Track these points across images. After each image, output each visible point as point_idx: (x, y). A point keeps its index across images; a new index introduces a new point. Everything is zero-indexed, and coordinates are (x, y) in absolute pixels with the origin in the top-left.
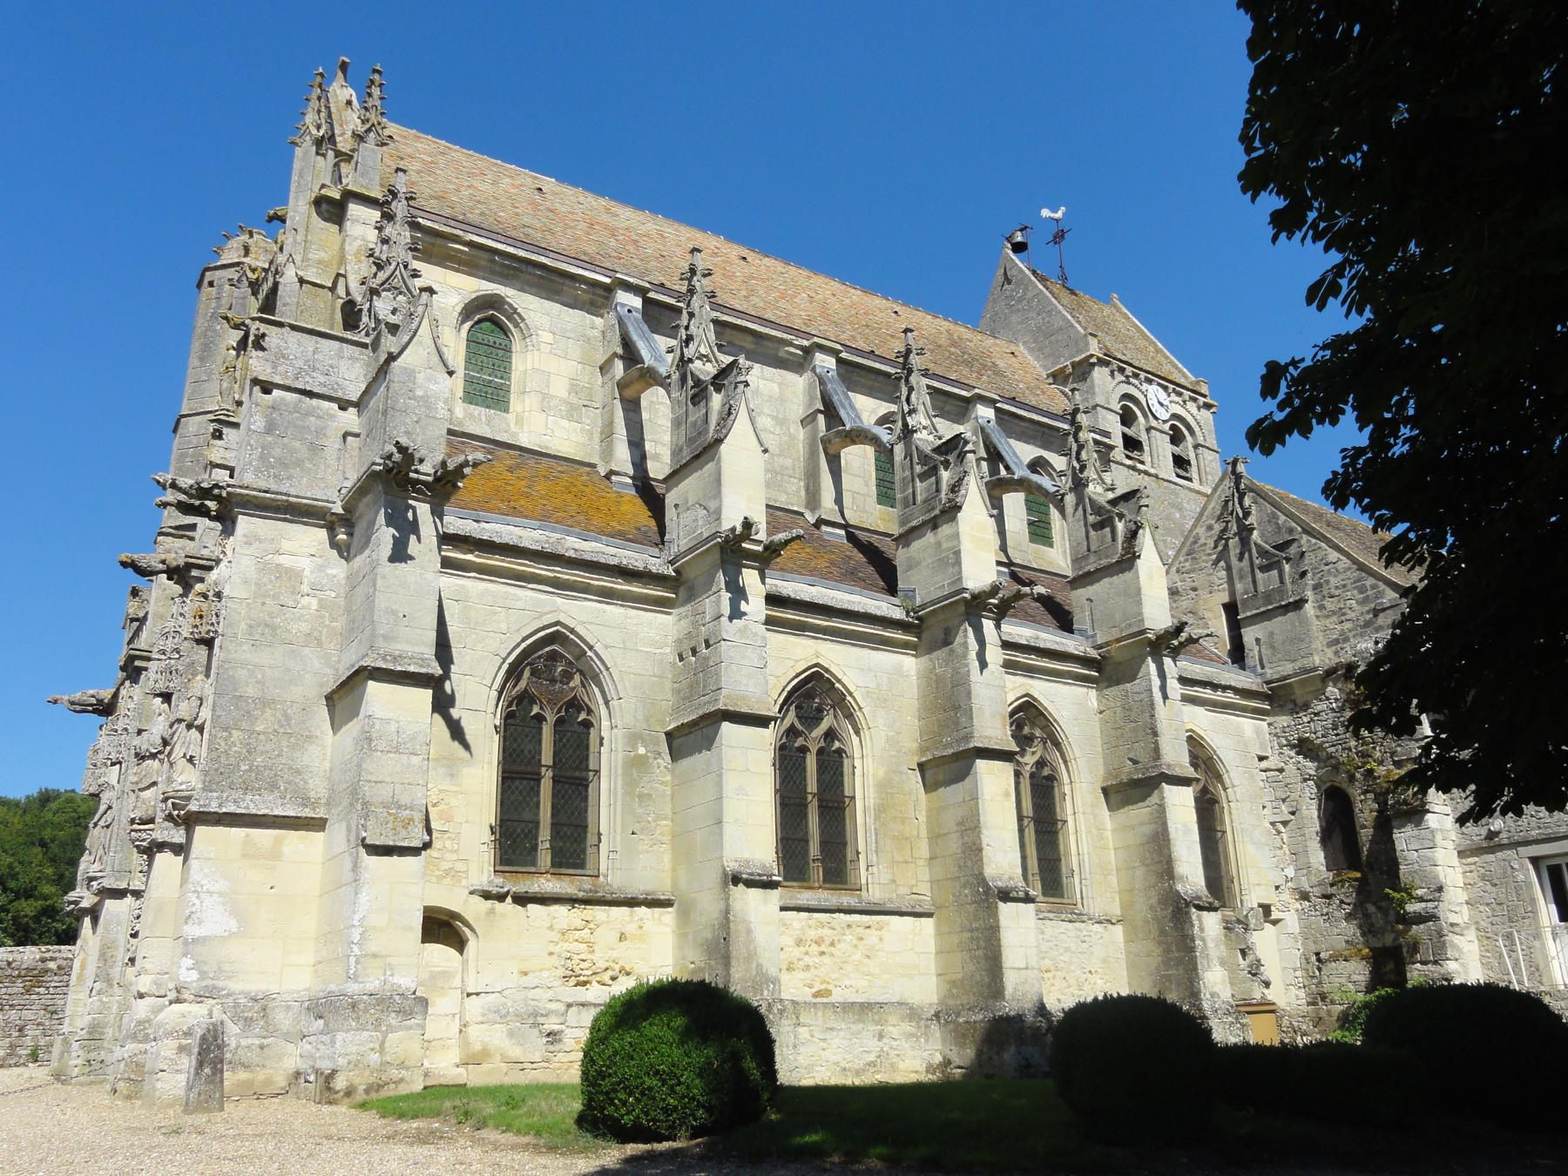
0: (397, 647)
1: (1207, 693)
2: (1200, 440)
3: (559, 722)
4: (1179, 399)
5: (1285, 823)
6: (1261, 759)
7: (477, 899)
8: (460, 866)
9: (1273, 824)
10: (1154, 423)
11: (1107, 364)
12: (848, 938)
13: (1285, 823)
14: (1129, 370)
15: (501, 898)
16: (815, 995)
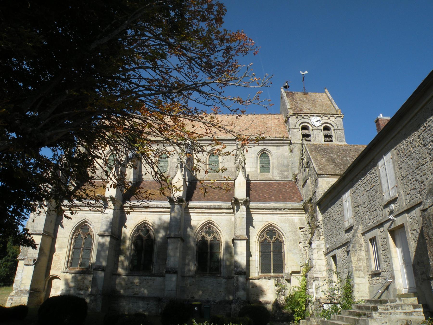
0: (37, 229)
1: (278, 211)
2: (336, 128)
3: (86, 238)
4: (326, 118)
5: (307, 247)
6: (301, 228)
7: (62, 273)
8: (60, 267)
9: (304, 247)
10: (315, 128)
11: (295, 115)
12: (144, 282)
13: (307, 247)
14: (303, 115)
15: (67, 273)
16: (134, 295)
